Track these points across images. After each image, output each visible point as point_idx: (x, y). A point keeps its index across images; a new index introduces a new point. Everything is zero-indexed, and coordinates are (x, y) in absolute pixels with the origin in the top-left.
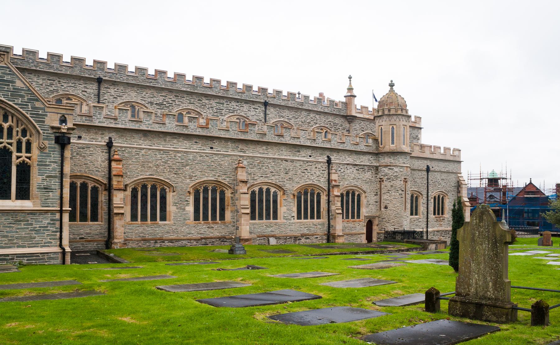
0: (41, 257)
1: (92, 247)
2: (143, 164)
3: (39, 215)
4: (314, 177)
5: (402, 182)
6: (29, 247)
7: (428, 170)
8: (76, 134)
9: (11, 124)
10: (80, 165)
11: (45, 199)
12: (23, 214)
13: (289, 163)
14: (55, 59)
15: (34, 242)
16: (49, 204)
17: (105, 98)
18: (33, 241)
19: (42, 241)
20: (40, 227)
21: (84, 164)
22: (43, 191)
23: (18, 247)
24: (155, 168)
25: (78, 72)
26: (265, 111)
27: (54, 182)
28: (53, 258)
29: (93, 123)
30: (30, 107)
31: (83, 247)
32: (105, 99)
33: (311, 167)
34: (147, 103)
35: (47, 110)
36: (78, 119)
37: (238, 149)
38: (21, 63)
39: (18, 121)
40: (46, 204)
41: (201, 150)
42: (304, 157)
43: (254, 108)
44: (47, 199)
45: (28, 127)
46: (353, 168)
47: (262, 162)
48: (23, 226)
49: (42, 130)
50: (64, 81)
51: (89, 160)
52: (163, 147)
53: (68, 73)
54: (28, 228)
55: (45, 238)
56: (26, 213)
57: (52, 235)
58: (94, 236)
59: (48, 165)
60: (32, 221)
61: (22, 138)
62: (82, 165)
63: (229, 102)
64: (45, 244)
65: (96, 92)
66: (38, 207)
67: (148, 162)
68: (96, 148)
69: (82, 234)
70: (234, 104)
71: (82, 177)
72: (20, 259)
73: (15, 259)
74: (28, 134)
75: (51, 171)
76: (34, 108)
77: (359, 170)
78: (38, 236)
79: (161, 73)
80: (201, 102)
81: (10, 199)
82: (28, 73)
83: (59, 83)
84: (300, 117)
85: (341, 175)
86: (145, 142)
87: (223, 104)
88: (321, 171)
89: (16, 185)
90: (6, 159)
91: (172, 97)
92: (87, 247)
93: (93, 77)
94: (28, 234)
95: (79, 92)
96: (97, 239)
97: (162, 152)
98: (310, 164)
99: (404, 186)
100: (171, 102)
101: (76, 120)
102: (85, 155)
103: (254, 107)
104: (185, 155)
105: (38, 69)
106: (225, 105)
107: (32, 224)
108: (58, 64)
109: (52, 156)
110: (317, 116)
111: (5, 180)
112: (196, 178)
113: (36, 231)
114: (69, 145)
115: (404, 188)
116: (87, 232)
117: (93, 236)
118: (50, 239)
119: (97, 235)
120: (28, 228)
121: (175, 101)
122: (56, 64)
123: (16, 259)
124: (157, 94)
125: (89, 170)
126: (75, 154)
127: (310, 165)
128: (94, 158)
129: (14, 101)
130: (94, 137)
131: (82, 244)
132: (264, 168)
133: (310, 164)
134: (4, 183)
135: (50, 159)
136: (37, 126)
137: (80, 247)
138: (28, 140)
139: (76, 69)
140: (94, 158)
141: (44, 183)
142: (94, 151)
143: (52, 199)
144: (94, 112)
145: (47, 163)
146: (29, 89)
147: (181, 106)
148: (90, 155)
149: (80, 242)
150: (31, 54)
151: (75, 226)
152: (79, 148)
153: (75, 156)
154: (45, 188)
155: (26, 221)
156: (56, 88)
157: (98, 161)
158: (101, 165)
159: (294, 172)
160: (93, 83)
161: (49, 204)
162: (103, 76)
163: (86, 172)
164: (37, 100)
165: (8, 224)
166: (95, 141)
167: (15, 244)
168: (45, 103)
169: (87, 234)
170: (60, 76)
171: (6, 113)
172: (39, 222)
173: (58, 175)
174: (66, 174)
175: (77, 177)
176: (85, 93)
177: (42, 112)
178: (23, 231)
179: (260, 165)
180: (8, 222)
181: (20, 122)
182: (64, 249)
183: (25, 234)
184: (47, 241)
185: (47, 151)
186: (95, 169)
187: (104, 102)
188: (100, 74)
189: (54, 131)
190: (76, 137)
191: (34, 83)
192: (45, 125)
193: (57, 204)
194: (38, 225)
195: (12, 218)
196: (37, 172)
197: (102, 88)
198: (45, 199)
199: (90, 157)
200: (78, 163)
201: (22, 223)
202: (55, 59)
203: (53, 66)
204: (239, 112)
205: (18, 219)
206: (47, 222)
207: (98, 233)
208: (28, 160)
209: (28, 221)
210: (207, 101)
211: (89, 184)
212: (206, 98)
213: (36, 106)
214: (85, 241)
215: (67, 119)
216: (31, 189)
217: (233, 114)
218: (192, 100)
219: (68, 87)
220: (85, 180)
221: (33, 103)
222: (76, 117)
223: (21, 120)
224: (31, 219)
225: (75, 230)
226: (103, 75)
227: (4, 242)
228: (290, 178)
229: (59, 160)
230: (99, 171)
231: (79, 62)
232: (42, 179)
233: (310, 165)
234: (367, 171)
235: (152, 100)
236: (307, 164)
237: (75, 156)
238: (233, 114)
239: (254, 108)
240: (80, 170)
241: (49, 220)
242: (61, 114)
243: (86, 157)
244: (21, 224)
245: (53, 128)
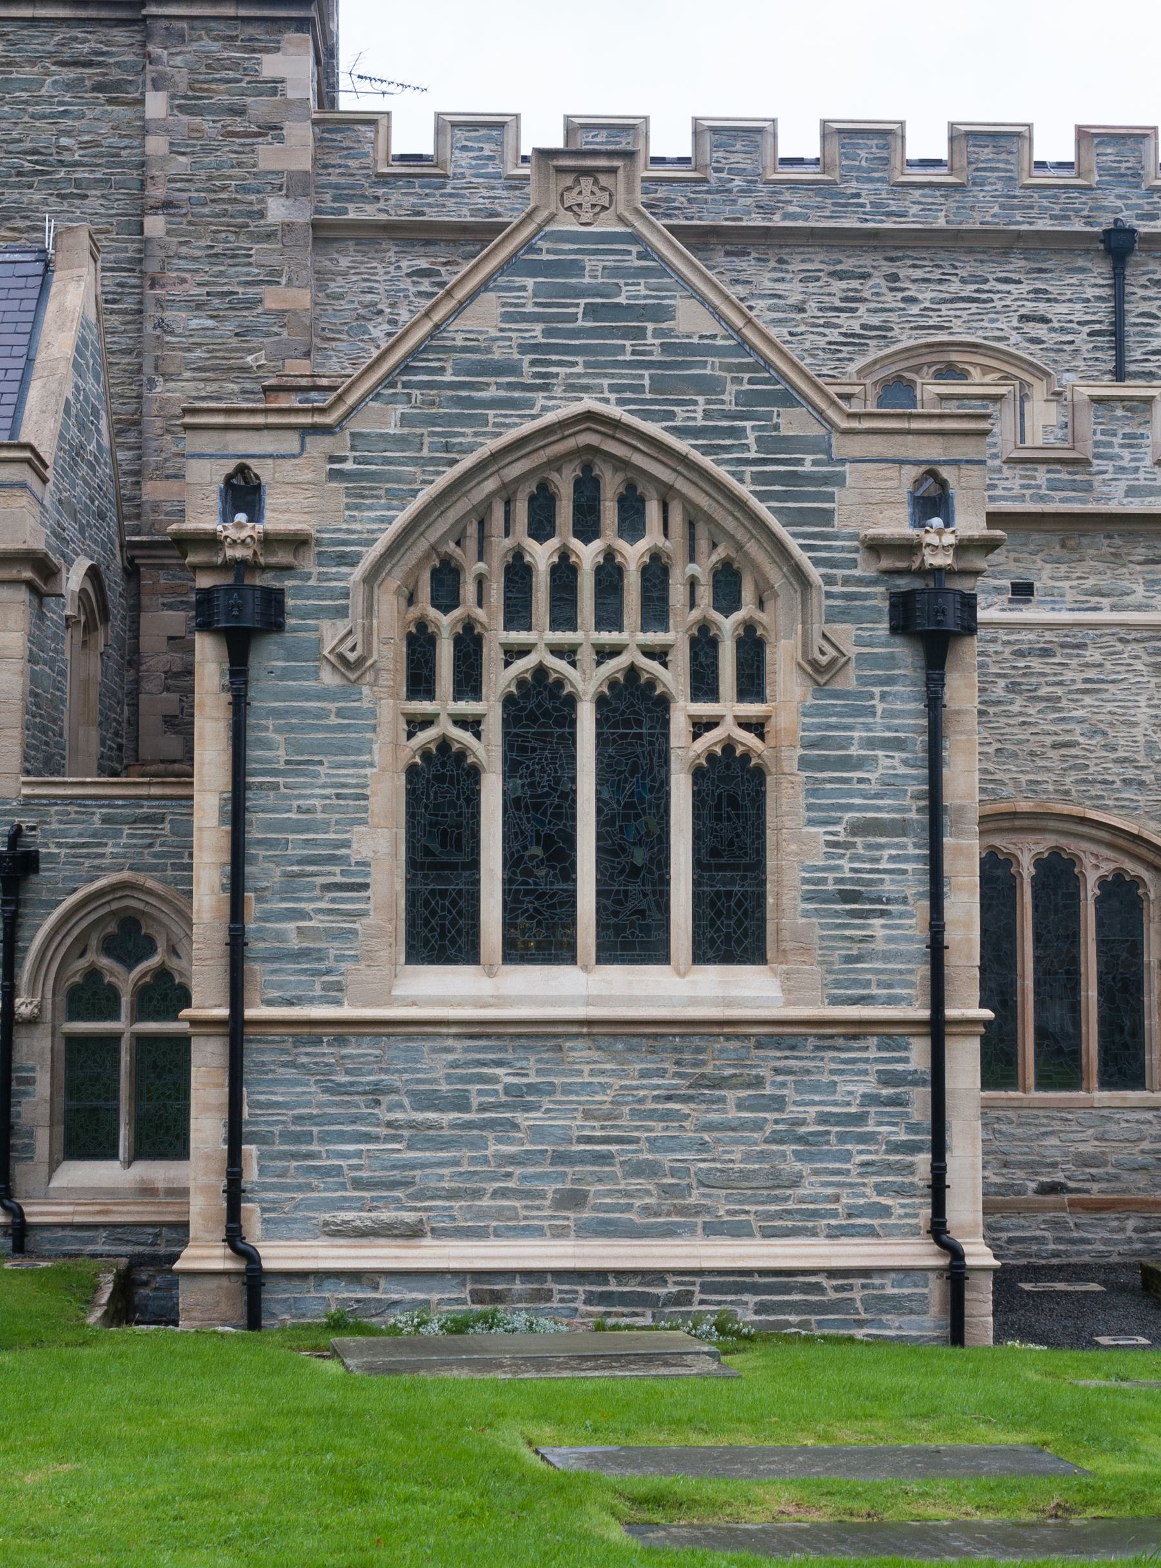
0: (833, 1295)
1: (1116, 1243)
3: (818, 1048)
6: (769, 1233)
8: (1002, 574)
9: (661, 541)
10: (1032, 754)
11: (849, 959)
12: (733, 1045)
14: (863, 154)
15: (790, 1205)
16: (867, 984)
18: (786, 1199)
19: (836, 1198)
20: (823, 1119)
21: (1055, 746)
22: (836, 914)
23: (713, 1230)
25: (996, 210)
27: (892, 859)
28: (897, 1305)
29: (1097, 500)
30: (751, 440)
31: (1057, 1240)
35: (842, 447)
36: (1007, 484)
38: (689, 200)
39: (691, 525)
40: (856, 983)
44: (858, 959)
45: (746, 555)
48: (733, 1114)
49: (817, 562)
50: (919, 274)
51: (1081, 721)
53: (941, 223)
54: (758, 1126)
55: (851, 1185)
56: (747, 1036)
57: (889, 1168)
58: (1125, 1175)
59: (859, 763)
60: (783, 1085)
61: (717, 616)
62: (1039, 750)
64: (850, 1216)
65: (1102, 313)
66: (810, 1003)
68: (1120, 647)
69: (1054, 1165)
71: (1043, 823)
72: (720, 1303)
73: (698, 1297)
74: (748, 594)
75: (877, 796)
76: (773, 444)
78: (816, 1172)
81: (665, 959)
82: (728, 254)
83: (892, 289)
89: (696, 883)
90: (639, 736)
92: (1083, 1241)
93: (1078, 226)
94: (762, 1156)
95: (1006, 325)
96: (1142, 1196)
101: (999, 492)
102: (1059, 691)
105: (777, 221)
107: (778, 1103)
108: (880, 180)
109: (880, 707)
111: (639, 857)
113: (801, 1139)
114: (968, 640)
116: (1083, 1148)
117: (1117, 1178)
118: (880, 1189)
119: (1143, 1168)
120: (758, 1126)
122: (871, 180)
123: (702, 1302)
125: (1085, 781)
126: (999, 690)
128: (1110, 707)
129: (671, 415)
130: (1105, 582)
131: (1055, 1225)
134: (635, 871)
135: (867, 727)
136: (793, 544)
137: (1041, 1240)
138: (749, 627)
139: (980, 195)
140: (1110, 707)
141: (838, 868)
142: (1108, 665)
143: (887, 957)
144: (1099, 437)
145: (854, 751)
146: (745, 341)
148: (1086, 692)
149: (1042, 1209)
150: (739, 147)
151: (1011, 1114)
152: (1020, 654)
153: (999, 703)
154: (848, 897)
155: (749, 1086)
156: (875, 320)
157: (1135, 724)
160: (1080, 263)
161: (867, 984)
162: (1140, 217)
163: (1067, 792)
164: (789, 398)
165: (656, 1099)
166: (1114, 608)
167: (697, 1213)
168: (831, 413)
169: (1084, 1161)
170: (896, 248)
171: (631, 487)
172: (816, 1088)
173: (913, 815)
174: (961, 809)
175: (1018, 823)
176: (1039, 330)
177: (815, 463)
178: (735, 1142)
180: (658, 1087)
181: (702, 531)
182: (955, 1253)
183: (747, 1157)
184: (861, 1201)
185: (849, 681)
186: (1116, 773)
187: (1149, 367)
188: (1119, 203)
189: (886, 563)
190: (999, 590)
191: (761, 304)
192: (835, 537)
193: (910, 985)
194: (813, 1110)
195: (675, 1069)
196: (802, 801)
197: (1135, 289)
198: (849, 959)
199: (1088, 700)
200: (1020, 742)
201: (731, 1095)
202: (863, 154)
203: (858, 195)
205: (708, 1069)
206: (861, 1089)
207: (1149, 1159)
208: (748, 739)
209: (759, 1082)
211: (1088, 861)
213: (784, 431)
214: (1072, 1203)
215: (955, 489)
216: (770, 900)
219: (944, 301)
220: (1063, 842)
221: (768, 416)
222: (1000, 471)
223: (710, 519)
224: (777, 1071)
225: (1013, 1137)
226: (1139, 206)
227: (638, 1203)
229: (914, 729)
230: (1142, 783)
231: (998, 149)
232: (829, 844)
237: (999, 703)
240: (1031, 782)
241: (872, 1078)
242: (917, 463)
243: (1064, 703)
245: (876, 547)
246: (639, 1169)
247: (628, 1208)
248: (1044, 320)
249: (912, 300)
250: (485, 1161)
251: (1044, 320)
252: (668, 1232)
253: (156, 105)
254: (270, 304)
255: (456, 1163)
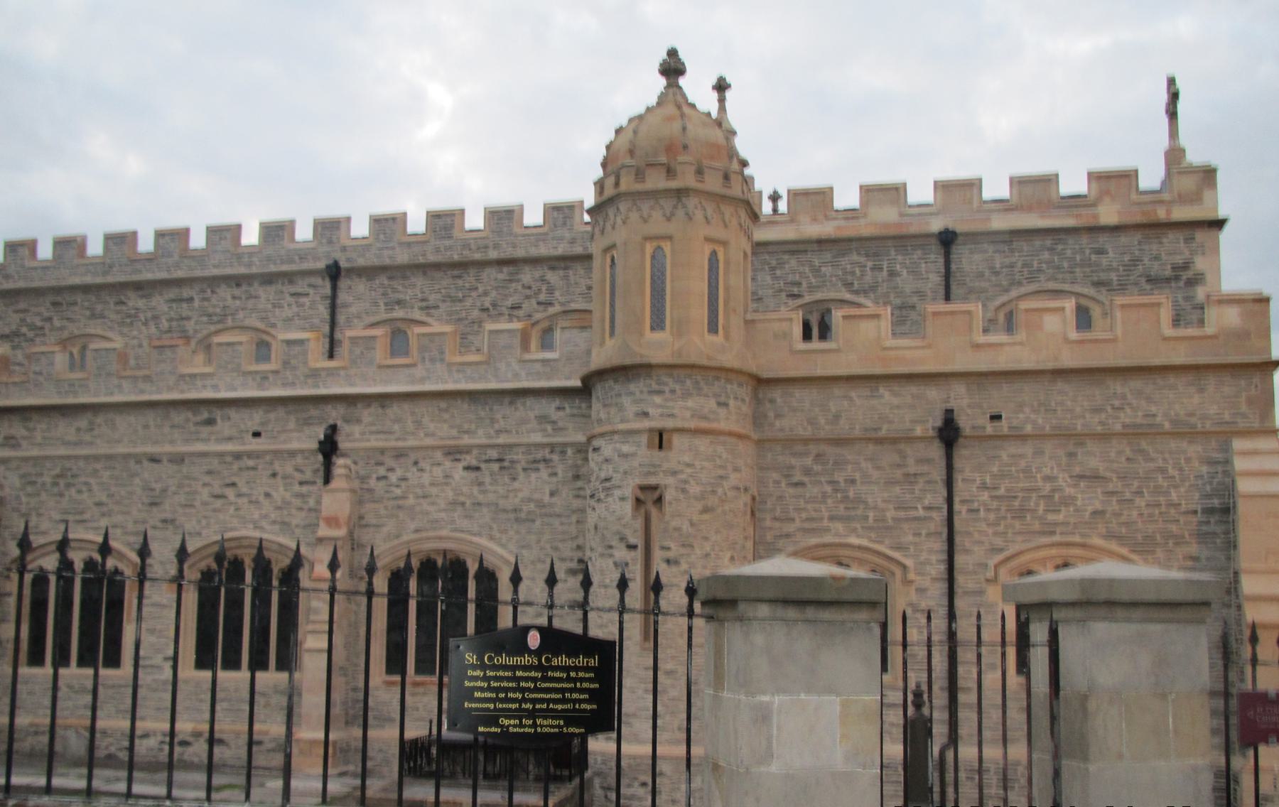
4: (263, 512)
5: (628, 507)
7: (949, 433)
13: (166, 469)
26: (334, 297)
33: (252, 473)
42: (230, 439)
43: (293, 295)
46: (448, 464)
47: (69, 474)
63: (209, 291)
70: (225, 293)
77: (478, 469)
79: (172, 238)
80: (124, 308)
84: (474, 294)
85: (388, 495)
87: (191, 300)
88: (297, 488)
91: (42, 309)
98: (251, 463)
99: (639, 524)
100: (39, 324)
103: (293, 289)
106: (196, 303)
110: (553, 277)
115: (641, 533)
127: (248, 468)
132: (73, 491)
133: (251, 463)
159: (182, 498)
179: (62, 482)
204: (241, 315)
210: (141, 303)
212: (140, 293)
217: (219, 326)
218: (99, 307)
228: (165, 521)
233: (248, 468)
234: (524, 469)
236: (235, 467)
238: (219, 326)
239: (293, 295)
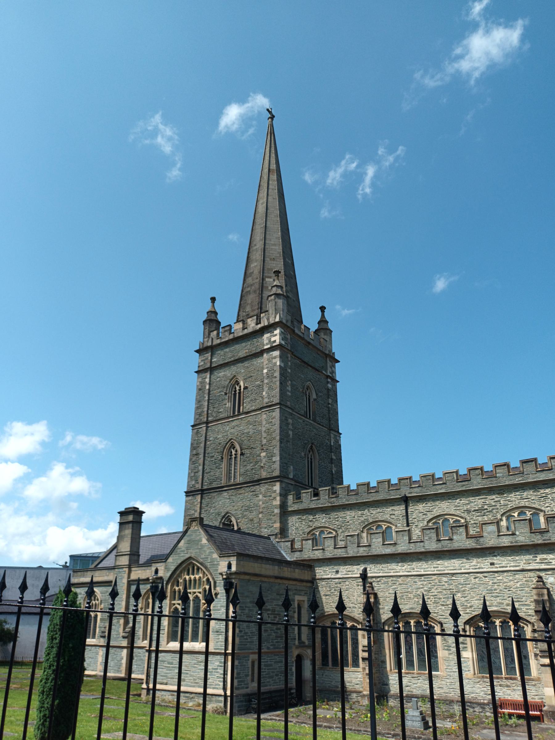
2: (402, 596)
8: (334, 569)
17: (414, 517)
24: (417, 600)
32: (414, 519)
34: (462, 513)
37: (536, 560)
41: (476, 569)
52: (424, 571)
67: (407, 592)
68: (351, 581)
81: (197, 641)
86: (403, 568)
97: (423, 578)
104: (454, 578)
112: (472, 609)
121: (499, 501)
124: (473, 498)
145: (219, 608)
147: (509, 506)
152: (336, 584)
154: (217, 632)
156: (366, 518)
158: (357, 600)
166: (351, 574)
176: (393, 517)
187: (413, 521)
190: (334, 572)
199: (347, 592)
235: (469, 507)
244: (201, 665)
246: (191, 676)
247: (189, 682)
248: (394, 515)
249: (372, 514)
250: (174, 673)
251: (394, 515)
252: (194, 686)
253: (261, 497)
254: (274, 527)
255: (171, 673)
